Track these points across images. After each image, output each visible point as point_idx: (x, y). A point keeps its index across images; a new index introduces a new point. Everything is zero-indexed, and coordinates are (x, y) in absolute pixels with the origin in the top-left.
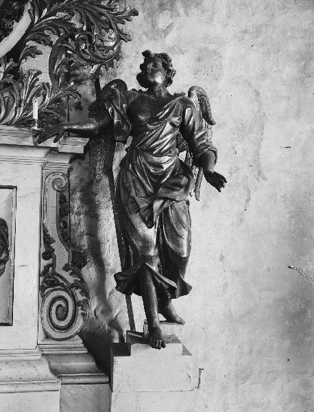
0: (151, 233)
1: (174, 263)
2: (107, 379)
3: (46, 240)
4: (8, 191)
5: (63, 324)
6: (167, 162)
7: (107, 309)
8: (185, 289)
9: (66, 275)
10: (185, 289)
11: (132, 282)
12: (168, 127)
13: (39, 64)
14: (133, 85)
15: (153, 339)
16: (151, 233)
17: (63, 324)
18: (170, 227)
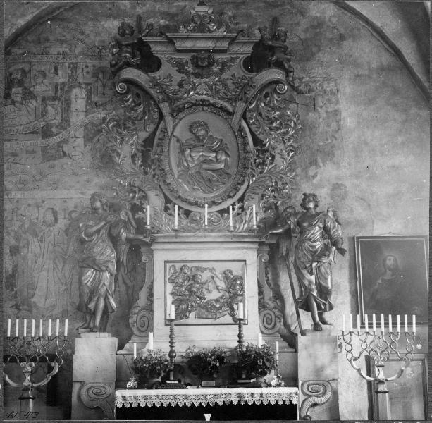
0: (313, 278)
2: (294, 350)
3: (260, 286)
4: (243, 263)
5: (270, 327)
6: (319, 245)
9: (270, 303)
11: (304, 304)
12: (317, 228)
14: (299, 209)
16: (313, 278)
17: (270, 327)
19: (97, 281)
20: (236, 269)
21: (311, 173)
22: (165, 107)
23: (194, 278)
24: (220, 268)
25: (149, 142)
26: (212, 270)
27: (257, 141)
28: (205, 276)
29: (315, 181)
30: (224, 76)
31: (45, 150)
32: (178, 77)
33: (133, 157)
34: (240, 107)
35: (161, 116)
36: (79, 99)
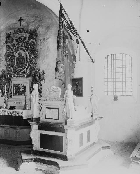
13: (28, 70)
20: (25, 84)
21: (44, 62)
22: (14, 50)
24: (23, 84)
26: (21, 85)
27: (30, 56)
29: (45, 63)
30: (24, 42)
32: (16, 43)
34: (26, 48)
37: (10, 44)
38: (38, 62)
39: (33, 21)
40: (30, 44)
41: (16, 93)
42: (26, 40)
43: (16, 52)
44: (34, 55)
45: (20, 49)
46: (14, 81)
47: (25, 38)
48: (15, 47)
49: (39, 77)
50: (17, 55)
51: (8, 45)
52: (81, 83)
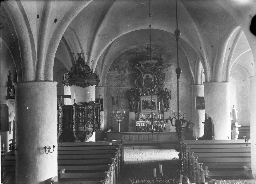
1: (168, 105)
7: (163, 109)
8: (169, 107)
10: (169, 107)
11: (165, 107)
14: (164, 91)
15: (167, 111)
18: (168, 102)
19: (132, 103)
22: (142, 73)
23: (147, 102)
25: (139, 79)
27: (157, 79)
28: (149, 102)
29: (168, 84)
31: (121, 79)
33: (137, 82)
34: (155, 73)
35: (141, 75)
36: (127, 71)
37: (138, 68)
38: (164, 83)
39: (154, 49)
40: (159, 69)
41: (145, 108)
42: (154, 66)
43: (144, 74)
44: (161, 78)
45: (148, 73)
46: (142, 98)
47: (153, 64)
48: (142, 70)
49: (169, 95)
50: (144, 77)
51: (136, 69)
52: (68, 90)
